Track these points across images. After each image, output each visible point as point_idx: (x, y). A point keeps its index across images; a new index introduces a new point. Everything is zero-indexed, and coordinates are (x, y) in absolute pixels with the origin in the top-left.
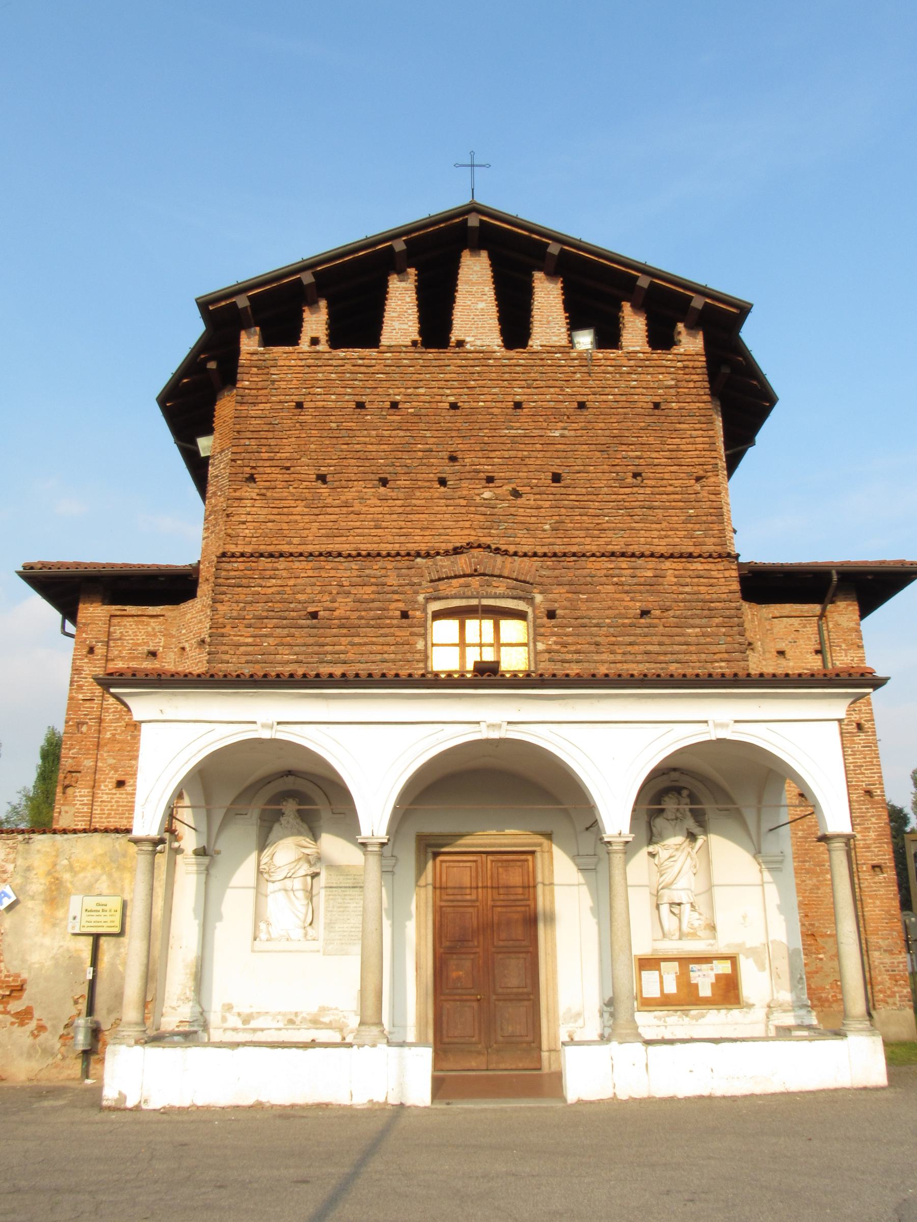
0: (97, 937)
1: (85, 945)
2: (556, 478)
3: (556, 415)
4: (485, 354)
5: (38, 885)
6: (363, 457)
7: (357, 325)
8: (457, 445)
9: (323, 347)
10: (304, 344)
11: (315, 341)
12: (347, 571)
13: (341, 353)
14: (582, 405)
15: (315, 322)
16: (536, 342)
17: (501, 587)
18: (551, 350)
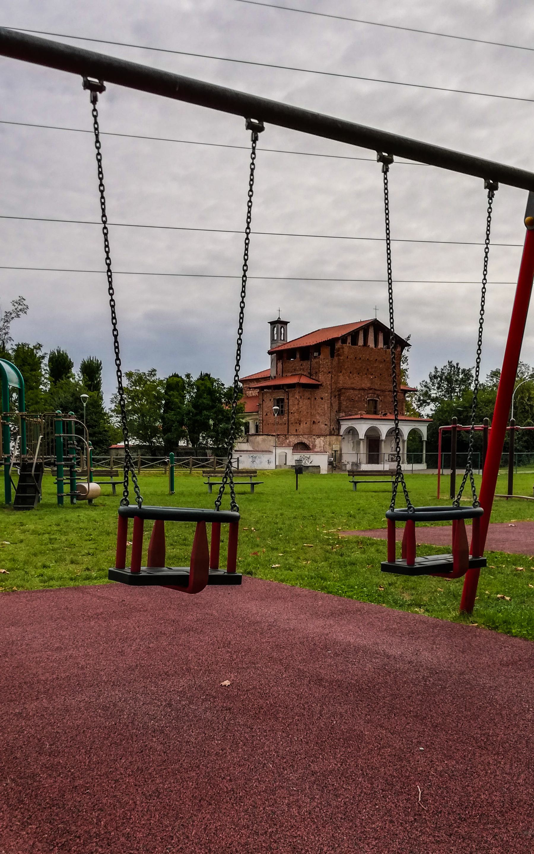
0: (335, 451)
1: (333, 452)
2: (381, 375)
3: (381, 362)
4: (372, 348)
5: (328, 443)
6: (356, 368)
7: (354, 342)
8: (369, 367)
9: (350, 345)
10: (348, 345)
11: (349, 343)
12: (357, 392)
13: (353, 346)
14: (385, 361)
15: (349, 340)
16: (379, 347)
17: (375, 396)
18: (381, 348)
